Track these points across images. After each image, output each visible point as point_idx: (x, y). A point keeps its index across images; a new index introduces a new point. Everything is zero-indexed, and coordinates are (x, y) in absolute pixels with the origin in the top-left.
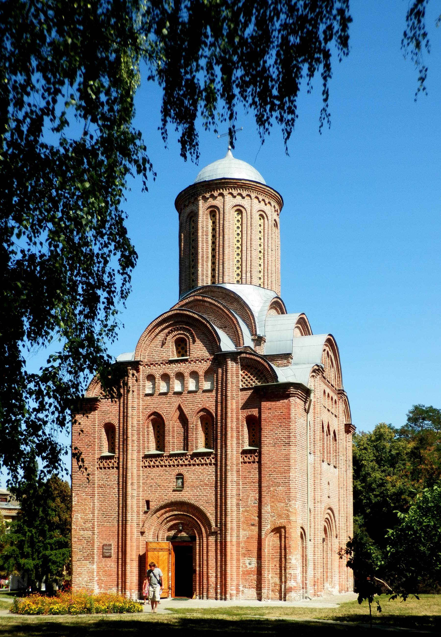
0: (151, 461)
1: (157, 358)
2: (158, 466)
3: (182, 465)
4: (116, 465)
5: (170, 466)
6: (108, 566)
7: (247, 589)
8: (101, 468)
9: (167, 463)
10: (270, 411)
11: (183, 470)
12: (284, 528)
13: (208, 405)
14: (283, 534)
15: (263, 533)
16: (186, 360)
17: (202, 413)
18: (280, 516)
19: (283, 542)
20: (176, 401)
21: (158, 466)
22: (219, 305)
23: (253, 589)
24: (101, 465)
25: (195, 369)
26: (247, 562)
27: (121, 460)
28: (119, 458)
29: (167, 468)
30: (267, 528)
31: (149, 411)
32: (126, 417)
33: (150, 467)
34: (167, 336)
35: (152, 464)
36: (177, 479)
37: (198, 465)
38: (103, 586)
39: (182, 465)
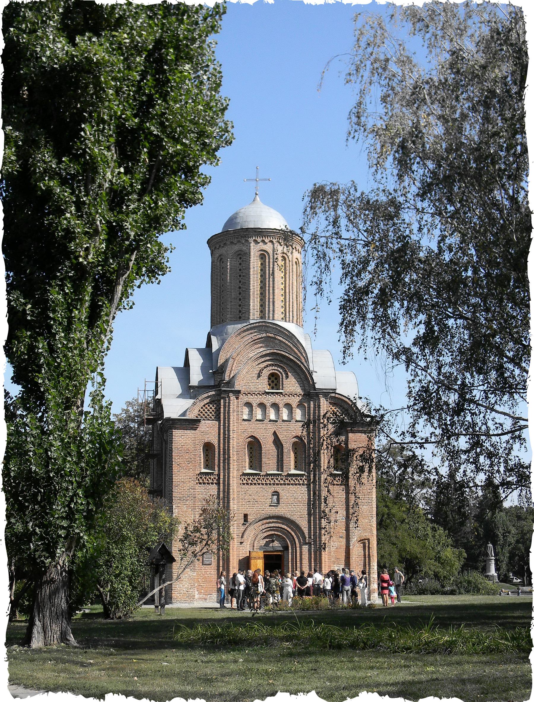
0: (249, 479)
1: (253, 389)
2: (255, 484)
3: (278, 484)
4: (215, 481)
5: (266, 484)
8: (200, 483)
10: (355, 443)
11: (278, 488)
12: (368, 540)
14: (367, 545)
15: (351, 544)
16: (281, 393)
17: (295, 440)
19: (367, 552)
20: (272, 428)
21: (255, 484)
22: (289, 344)
24: (201, 481)
27: (222, 477)
28: (219, 475)
29: (264, 486)
31: (246, 435)
32: (227, 439)
33: (248, 484)
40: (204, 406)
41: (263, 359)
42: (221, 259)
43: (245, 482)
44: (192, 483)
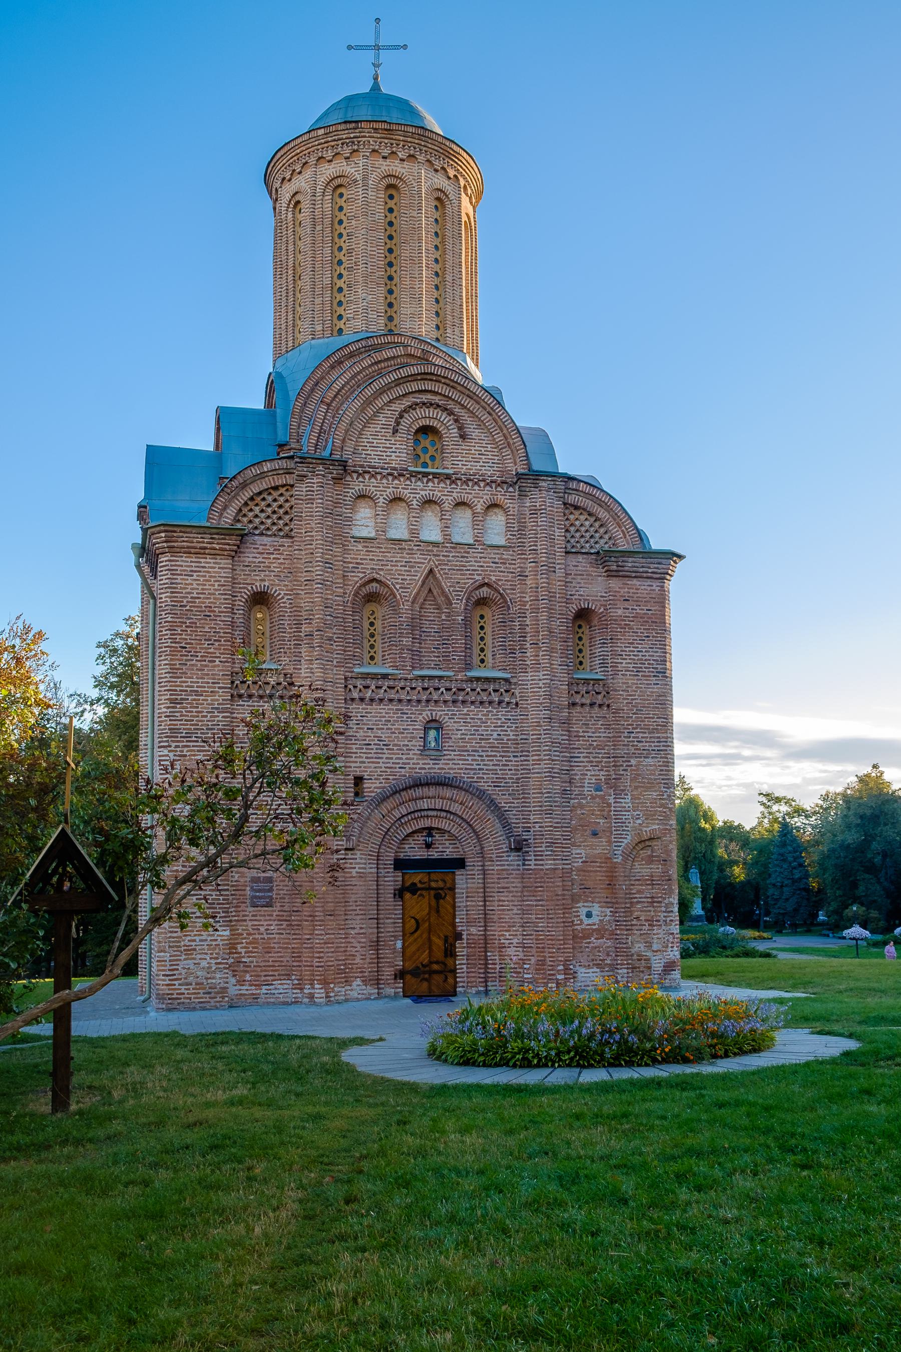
2: (381, 700)
6: (262, 929)
7: (583, 970)
9: (403, 696)
11: (440, 712)
13: (493, 578)
16: (448, 477)
18: (649, 816)
23: (595, 970)
25: (466, 498)
26: (583, 912)
30: (626, 841)
33: (362, 700)
34: (401, 417)
35: (369, 694)
36: (426, 730)
37: (472, 703)
38: (248, 978)
39: (436, 701)
40: (252, 499)
41: (400, 391)
42: (298, 202)
43: (355, 695)
44: (221, 696)
